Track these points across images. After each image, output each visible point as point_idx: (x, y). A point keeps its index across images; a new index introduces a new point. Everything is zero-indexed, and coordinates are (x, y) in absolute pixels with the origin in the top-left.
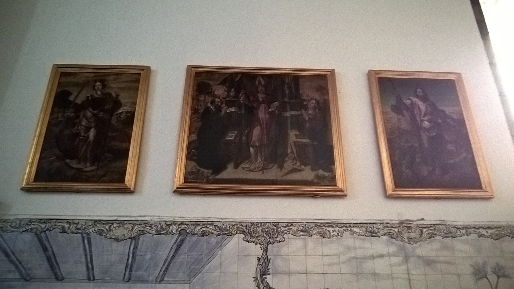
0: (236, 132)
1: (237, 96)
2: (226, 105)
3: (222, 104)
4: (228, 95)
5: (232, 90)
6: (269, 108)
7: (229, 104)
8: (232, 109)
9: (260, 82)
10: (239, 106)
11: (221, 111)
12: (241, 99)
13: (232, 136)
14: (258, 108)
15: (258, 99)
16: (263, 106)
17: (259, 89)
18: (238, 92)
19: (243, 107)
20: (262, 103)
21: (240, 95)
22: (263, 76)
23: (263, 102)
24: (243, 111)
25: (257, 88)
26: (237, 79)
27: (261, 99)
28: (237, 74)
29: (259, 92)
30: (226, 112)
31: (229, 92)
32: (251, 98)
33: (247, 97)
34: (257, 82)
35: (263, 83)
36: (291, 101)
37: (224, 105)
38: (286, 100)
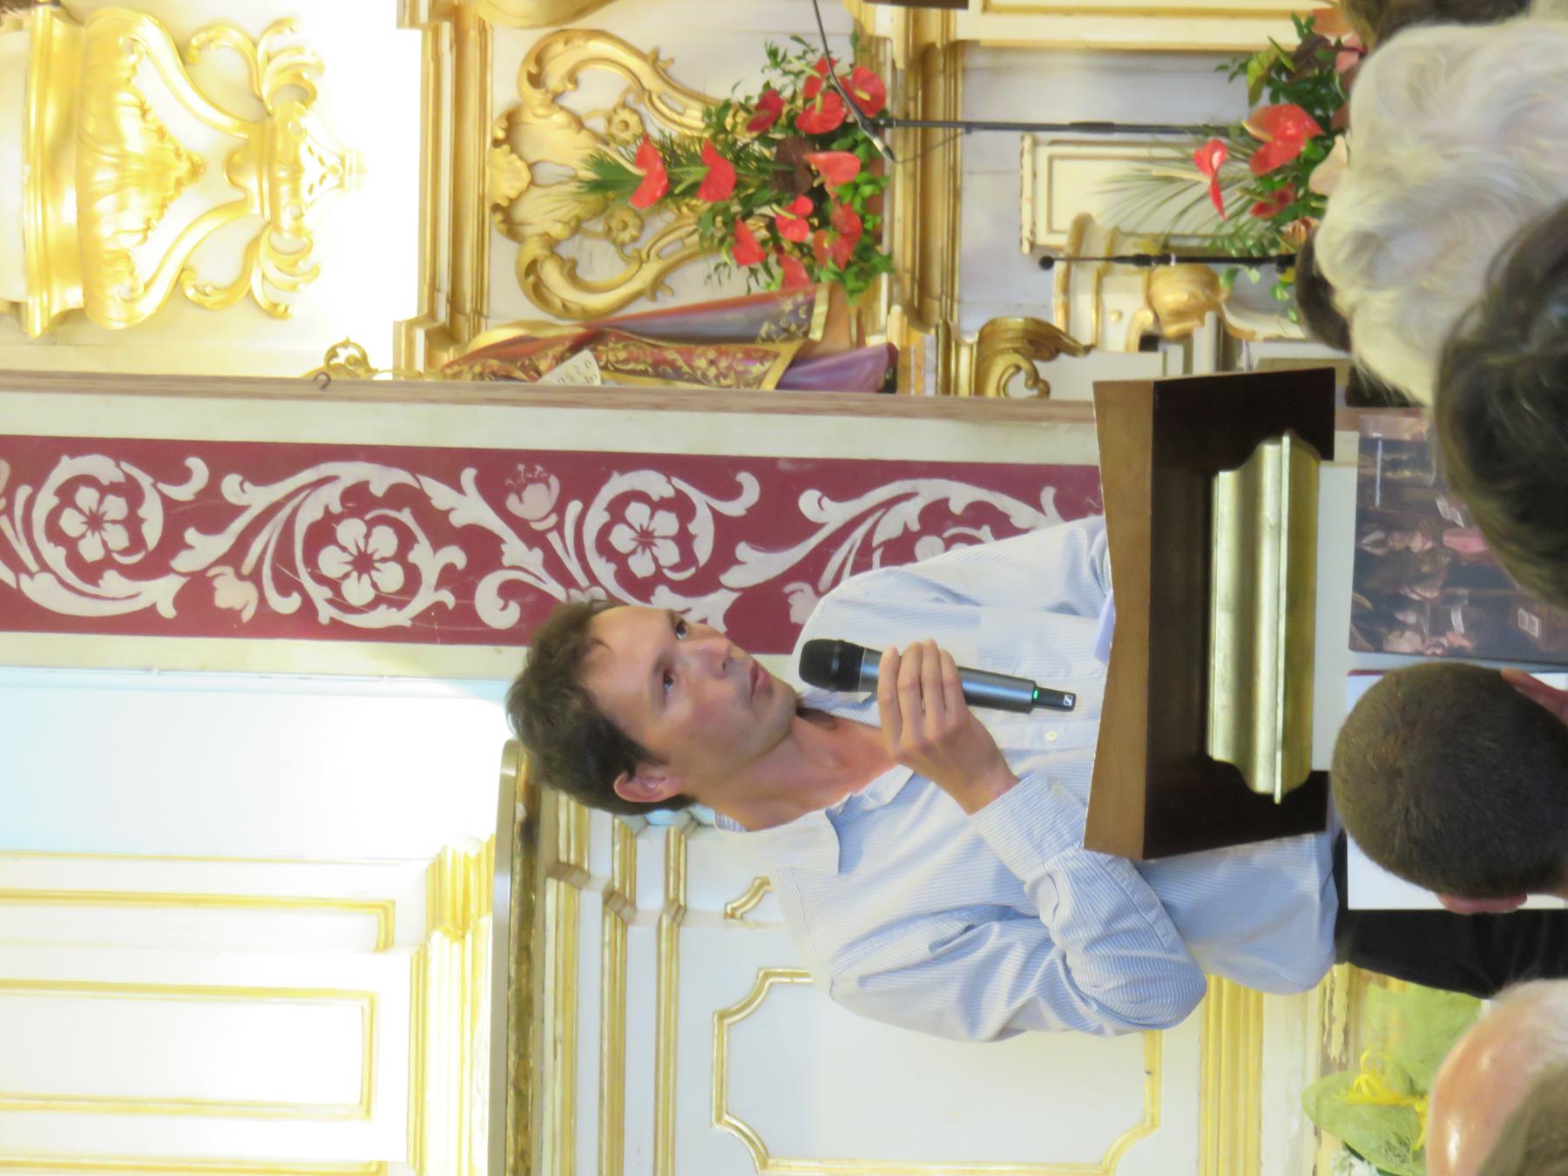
0: (1522, 612)
1: (1419, 606)
2: (1443, 634)
3: (1440, 645)
4: (1417, 629)
5: (1400, 617)
6: (1453, 525)
7: (1440, 625)
8: (1457, 619)
9: (1377, 544)
10: (1451, 600)
11: (1462, 648)
12: (1428, 595)
13: (1532, 622)
14: (1456, 555)
15: (1429, 552)
16: (1451, 541)
17: (1399, 546)
18: (1403, 603)
19: (1450, 590)
20: (1442, 545)
21: (1415, 597)
22: (1360, 534)
23: (1437, 538)
24: (1463, 592)
25: (1394, 553)
26: (1367, 604)
27: (1429, 545)
28: (1356, 605)
29: (1408, 549)
30: (1464, 636)
31: (1403, 627)
32: (1426, 569)
33: (1421, 579)
34: (1379, 552)
35: (1377, 535)
36: (1434, 465)
37: (1444, 641)
38: (1431, 478)
